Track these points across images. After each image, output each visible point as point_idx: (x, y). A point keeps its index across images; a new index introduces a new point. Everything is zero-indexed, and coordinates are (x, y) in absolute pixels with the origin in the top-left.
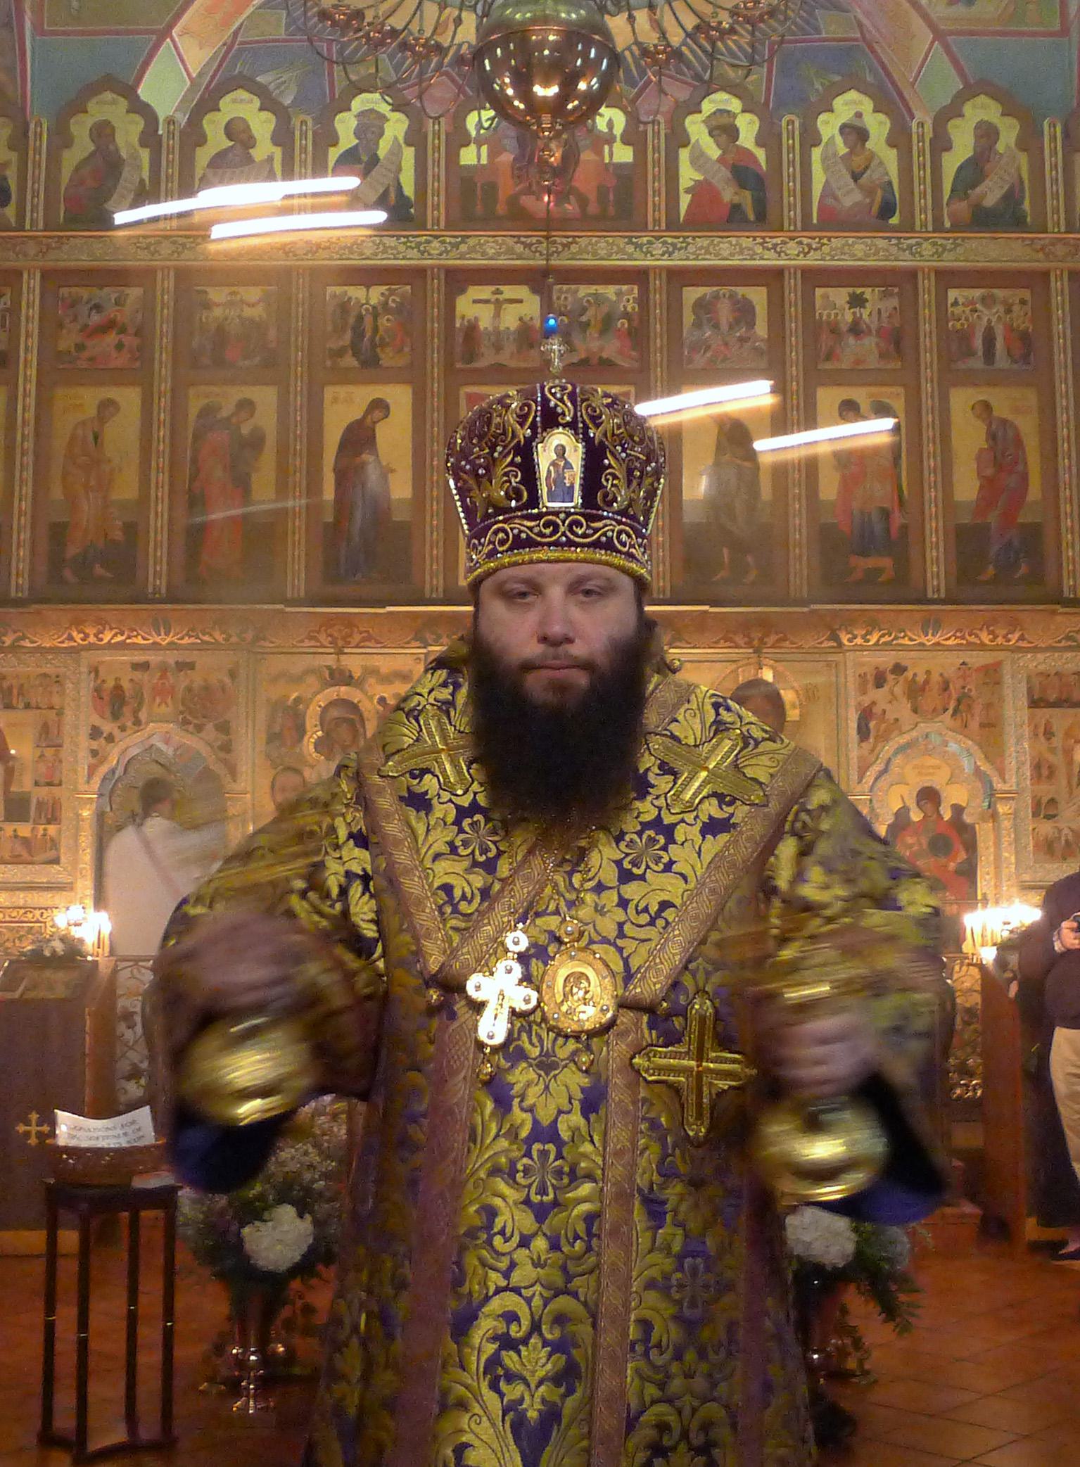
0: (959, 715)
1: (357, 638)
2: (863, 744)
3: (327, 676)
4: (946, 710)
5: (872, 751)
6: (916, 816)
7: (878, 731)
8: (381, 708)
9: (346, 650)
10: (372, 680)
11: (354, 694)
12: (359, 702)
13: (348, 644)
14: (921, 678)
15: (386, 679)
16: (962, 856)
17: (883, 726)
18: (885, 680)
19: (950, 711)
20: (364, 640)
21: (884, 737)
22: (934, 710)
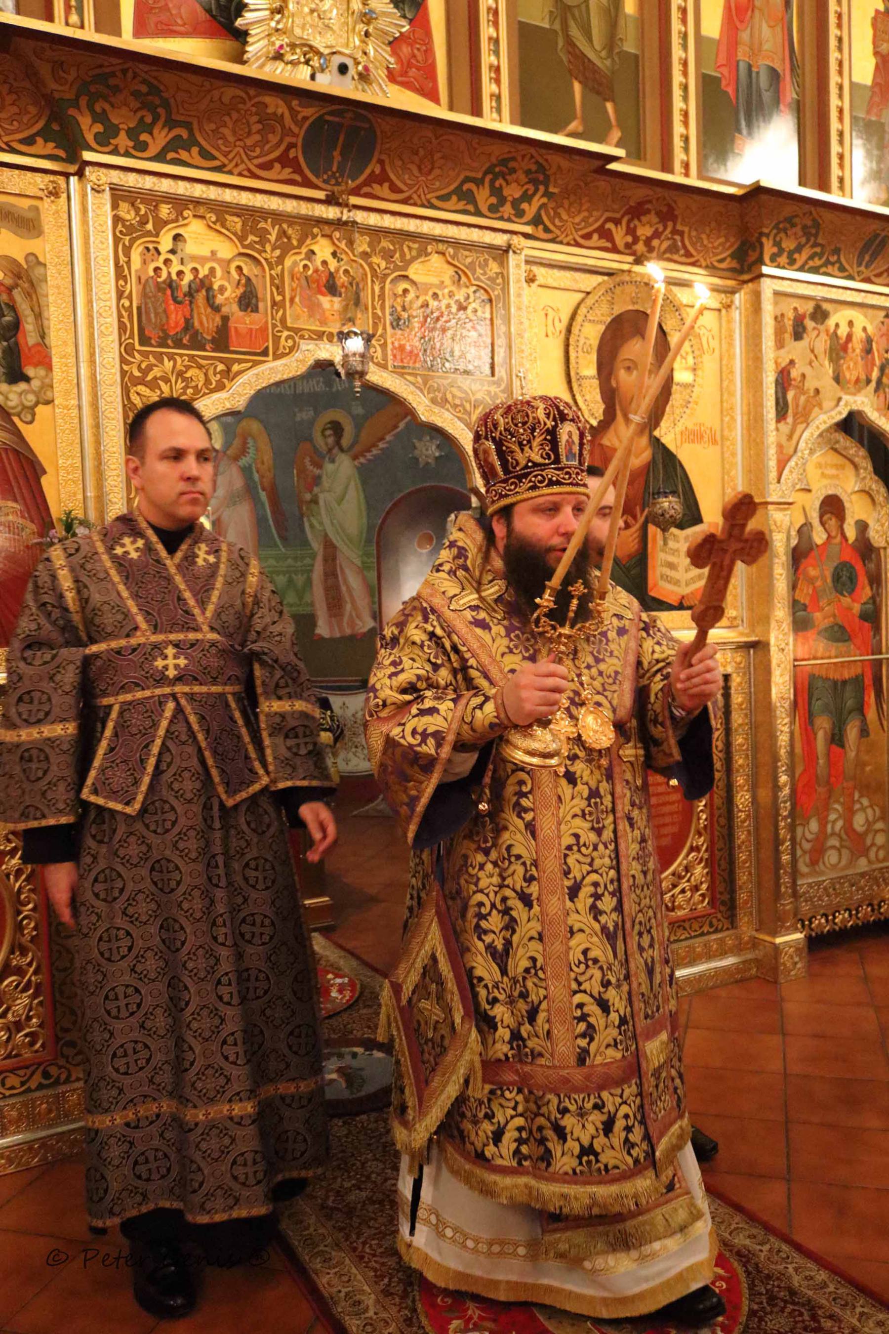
0: (881, 391)
2: (782, 425)
4: (868, 381)
5: (790, 437)
6: (819, 536)
7: (797, 406)
14: (843, 331)
16: (867, 592)
17: (803, 399)
18: (804, 329)
19: (873, 384)
21: (804, 417)
22: (857, 381)
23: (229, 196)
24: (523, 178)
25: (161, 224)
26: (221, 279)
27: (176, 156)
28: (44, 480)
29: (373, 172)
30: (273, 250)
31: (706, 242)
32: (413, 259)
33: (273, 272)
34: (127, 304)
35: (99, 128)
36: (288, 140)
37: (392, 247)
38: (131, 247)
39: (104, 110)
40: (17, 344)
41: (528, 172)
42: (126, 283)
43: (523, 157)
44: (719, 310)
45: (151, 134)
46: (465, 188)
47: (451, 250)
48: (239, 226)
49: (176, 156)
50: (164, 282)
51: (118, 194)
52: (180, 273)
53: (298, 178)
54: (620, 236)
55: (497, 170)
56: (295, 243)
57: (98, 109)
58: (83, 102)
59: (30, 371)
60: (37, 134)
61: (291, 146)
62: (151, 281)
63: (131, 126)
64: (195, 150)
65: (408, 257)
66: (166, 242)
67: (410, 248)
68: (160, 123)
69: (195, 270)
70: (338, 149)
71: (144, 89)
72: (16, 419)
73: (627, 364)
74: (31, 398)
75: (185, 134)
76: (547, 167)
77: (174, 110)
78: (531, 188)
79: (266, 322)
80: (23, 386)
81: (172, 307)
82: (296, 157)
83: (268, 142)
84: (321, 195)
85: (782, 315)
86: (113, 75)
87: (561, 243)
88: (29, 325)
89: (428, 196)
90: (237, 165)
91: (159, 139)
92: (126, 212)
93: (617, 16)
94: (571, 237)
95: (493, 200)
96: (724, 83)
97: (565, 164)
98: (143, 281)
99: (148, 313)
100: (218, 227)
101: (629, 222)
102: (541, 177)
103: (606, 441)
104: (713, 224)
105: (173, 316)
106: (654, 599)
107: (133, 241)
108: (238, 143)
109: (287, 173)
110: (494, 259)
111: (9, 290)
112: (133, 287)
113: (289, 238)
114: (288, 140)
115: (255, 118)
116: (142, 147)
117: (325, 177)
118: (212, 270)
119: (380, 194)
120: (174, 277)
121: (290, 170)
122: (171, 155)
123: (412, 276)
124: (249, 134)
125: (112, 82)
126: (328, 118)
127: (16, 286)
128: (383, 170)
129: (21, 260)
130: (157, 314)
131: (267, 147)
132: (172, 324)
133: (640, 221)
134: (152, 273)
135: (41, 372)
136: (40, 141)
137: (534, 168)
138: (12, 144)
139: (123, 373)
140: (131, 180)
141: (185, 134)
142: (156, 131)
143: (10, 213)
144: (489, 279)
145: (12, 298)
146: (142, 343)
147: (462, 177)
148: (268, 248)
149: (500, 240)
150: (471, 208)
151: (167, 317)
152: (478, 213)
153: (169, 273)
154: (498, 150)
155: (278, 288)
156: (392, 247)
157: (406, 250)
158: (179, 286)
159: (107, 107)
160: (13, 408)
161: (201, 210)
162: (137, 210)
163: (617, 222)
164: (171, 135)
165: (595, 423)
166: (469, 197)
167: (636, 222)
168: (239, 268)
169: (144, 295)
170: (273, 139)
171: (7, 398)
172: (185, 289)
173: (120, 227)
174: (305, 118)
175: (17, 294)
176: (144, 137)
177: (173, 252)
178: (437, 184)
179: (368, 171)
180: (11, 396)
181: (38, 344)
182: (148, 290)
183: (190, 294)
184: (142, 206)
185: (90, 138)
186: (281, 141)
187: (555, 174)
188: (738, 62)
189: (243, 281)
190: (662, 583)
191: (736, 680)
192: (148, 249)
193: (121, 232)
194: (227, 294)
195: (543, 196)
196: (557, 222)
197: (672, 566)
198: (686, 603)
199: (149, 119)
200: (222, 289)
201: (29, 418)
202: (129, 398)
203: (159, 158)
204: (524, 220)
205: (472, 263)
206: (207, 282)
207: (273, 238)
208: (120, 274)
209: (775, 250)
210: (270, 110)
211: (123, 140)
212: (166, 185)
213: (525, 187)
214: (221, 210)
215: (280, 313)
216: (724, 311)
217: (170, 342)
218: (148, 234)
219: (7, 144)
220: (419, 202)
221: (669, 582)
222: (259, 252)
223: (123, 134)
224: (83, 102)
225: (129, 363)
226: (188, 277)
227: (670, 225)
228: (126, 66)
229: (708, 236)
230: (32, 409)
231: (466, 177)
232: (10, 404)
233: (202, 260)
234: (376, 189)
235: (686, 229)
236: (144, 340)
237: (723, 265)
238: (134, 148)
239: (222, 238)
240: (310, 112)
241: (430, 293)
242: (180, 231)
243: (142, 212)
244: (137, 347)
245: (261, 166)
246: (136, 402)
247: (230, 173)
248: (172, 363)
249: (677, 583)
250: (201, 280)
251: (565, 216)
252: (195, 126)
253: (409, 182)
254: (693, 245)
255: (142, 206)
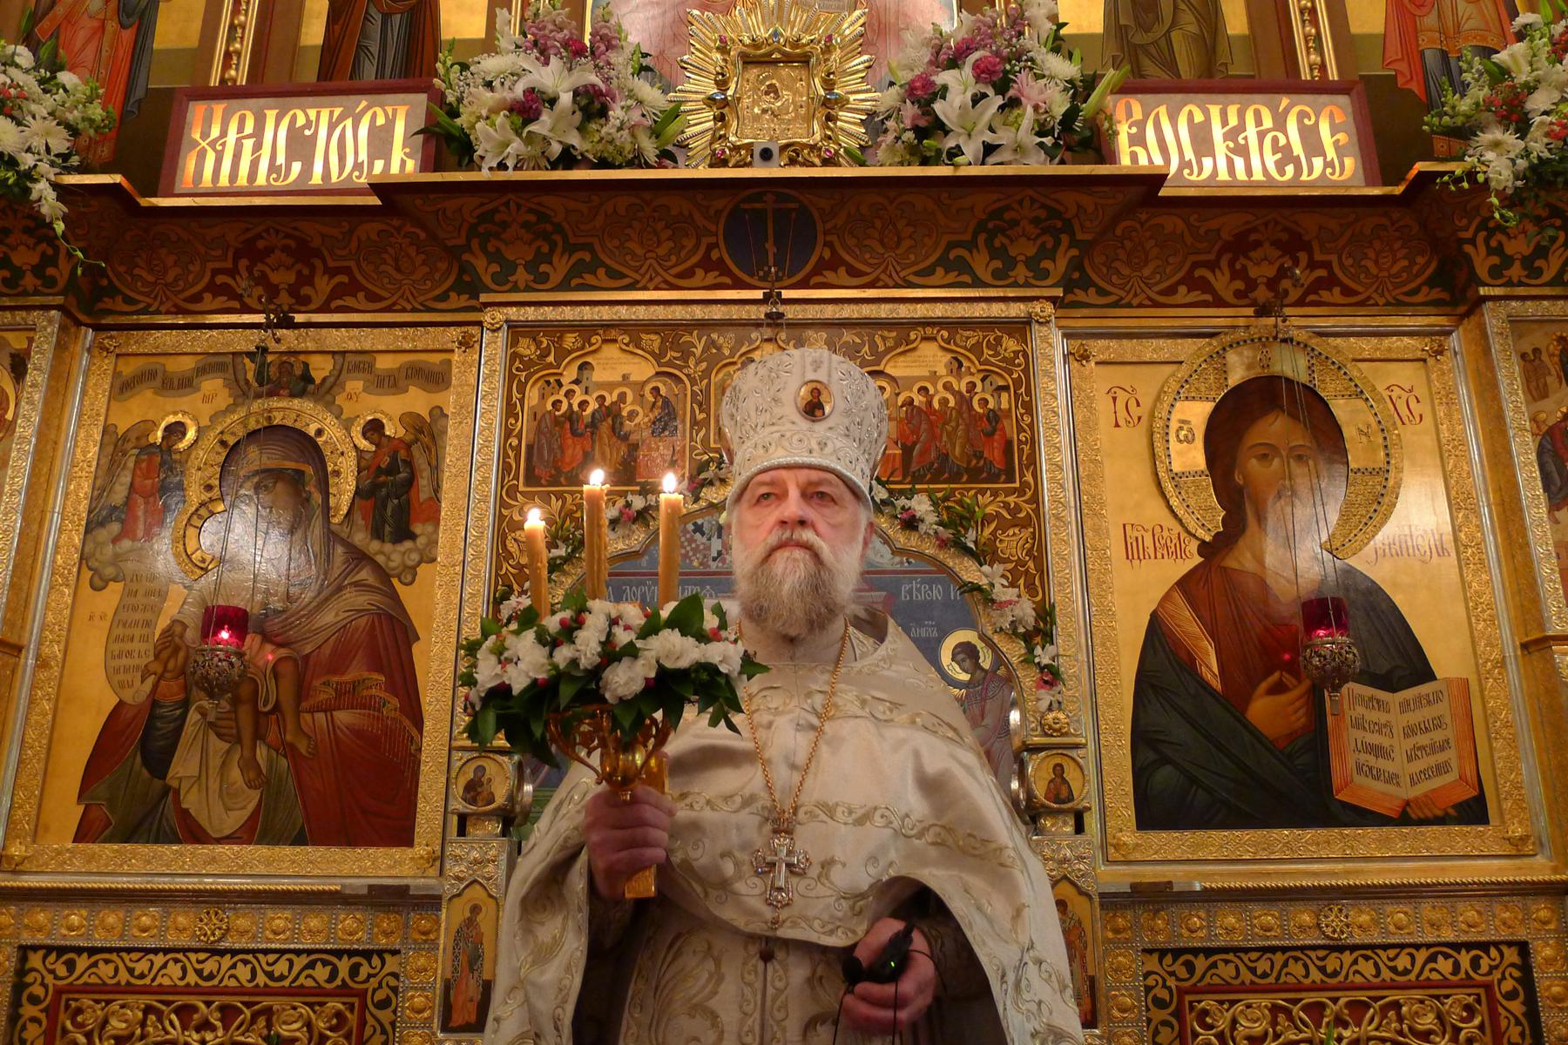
1: (323, 285)
3: (250, 376)
8: (364, 444)
9: (299, 318)
10: (355, 385)
11: (309, 416)
12: (320, 432)
13: (303, 303)
15: (390, 383)
20: (337, 292)
23: (641, 313)
24: (1032, 230)
25: (562, 354)
26: (632, 404)
27: (581, 281)
28: (416, 649)
29: (821, 258)
30: (697, 364)
31: (1374, 271)
32: (888, 350)
33: (695, 388)
34: (515, 442)
35: (495, 268)
36: (705, 241)
37: (858, 340)
38: (526, 382)
39: (498, 250)
40: (408, 501)
41: (1035, 221)
42: (517, 421)
43: (1020, 203)
44: (1424, 360)
45: (551, 263)
46: (952, 256)
47: (945, 334)
48: (656, 345)
49: (581, 281)
50: (562, 415)
51: (516, 330)
52: (583, 404)
53: (728, 280)
54: (1221, 282)
55: (990, 225)
56: (727, 352)
57: (491, 249)
58: (475, 244)
59: (417, 528)
60: (450, 289)
61: (710, 248)
62: (547, 416)
63: (529, 258)
64: (601, 272)
65: (881, 348)
66: (570, 374)
67: (884, 339)
68: (559, 250)
69: (602, 398)
70: (771, 240)
71: (532, 218)
72: (395, 581)
73: (1263, 451)
74: (415, 557)
75: (587, 257)
76: (1062, 209)
77: (570, 234)
78: (1049, 241)
79: (684, 446)
80: (408, 544)
81: (570, 441)
82: (721, 260)
83: (683, 247)
84: (758, 294)
85: (1536, 351)
86: (495, 210)
87: (1129, 306)
88: (423, 482)
89: (902, 274)
90: (651, 279)
91: (561, 266)
92: (526, 348)
93: (1215, 39)
94: (1144, 296)
95: (997, 264)
96: (1401, 81)
97: (1086, 200)
98: (538, 417)
99: (540, 449)
100: (631, 348)
101: (1231, 264)
102: (1059, 224)
103: (1231, 563)
104: (1377, 244)
105: (569, 452)
106: (1344, 805)
107: (527, 379)
108: (648, 255)
109: (712, 277)
110: (1010, 336)
111: (409, 446)
112: (524, 424)
113: (719, 348)
114: (705, 241)
115: (660, 225)
116: (542, 279)
117: (761, 273)
118: (622, 397)
119: (836, 282)
120: (576, 408)
121: (717, 273)
122: (574, 282)
123: (888, 370)
124: (659, 244)
125: (497, 217)
126: (742, 206)
127: (417, 440)
128: (834, 252)
129: (425, 414)
130: (551, 450)
131: (683, 254)
132: (567, 460)
133: (1250, 259)
134: (549, 407)
135: (429, 528)
136: (453, 295)
137: (1042, 214)
138: (427, 303)
139: (501, 517)
140: (531, 314)
141: (587, 257)
142: (555, 260)
143: (421, 369)
144: (1004, 360)
145: (409, 453)
146: (528, 483)
147: (943, 244)
148: (692, 362)
149: (1016, 310)
150: (967, 279)
151: (563, 452)
152: (978, 283)
153: (570, 405)
154: (982, 202)
155: (700, 405)
156: (858, 340)
157: (878, 340)
158: (580, 417)
159: (503, 247)
160: (393, 569)
161: (613, 334)
162: (538, 344)
163: (1213, 266)
164: (573, 260)
165: (1208, 539)
166: (963, 267)
167: (1242, 260)
168: (656, 390)
169: (539, 431)
170: (689, 243)
171: (389, 559)
172: (588, 420)
173: (517, 364)
174: (718, 212)
175: (416, 450)
176: (543, 268)
177: (577, 382)
178: (912, 257)
179: (813, 260)
180: (395, 556)
181: (431, 499)
182: (543, 425)
183: (594, 424)
184: (544, 340)
185: (487, 280)
186: (697, 246)
187: (1077, 216)
188: (1422, 54)
189: (660, 403)
190: (1360, 780)
191: (1543, 952)
192: (548, 383)
193: (518, 369)
194: (637, 420)
195: (1070, 247)
196: (1114, 279)
197: (1378, 751)
198: (1414, 813)
199: (545, 249)
200: (632, 415)
201: (409, 578)
202: (504, 546)
203: (564, 286)
204: (1049, 282)
205: (979, 344)
206: (615, 408)
207: (698, 351)
208: (510, 411)
209: (1495, 260)
210: (674, 212)
211: (521, 275)
212: (568, 313)
213: (1039, 242)
214: (633, 329)
215: (702, 434)
216: (1431, 361)
217: (562, 480)
218: (550, 366)
219: (421, 304)
220: (891, 283)
221: (1377, 778)
222: (680, 368)
223: (521, 270)
224: (475, 244)
225: (508, 506)
226: (593, 406)
227: (1303, 257)
228: (504, 199)
229: (1376, 262)
230: (413, 570)
231: (949, 243)
232: (392, 564)
233: (610, 386)
234: (830, 276)
235: (1334, 259)
236: (531, 479)
237: (1419, 298)
238: (534, 281)
239: (637, 360)
240: (721, 203)
241: (915, 389)
242: (589, 359)
243: (544, 345)
244: (521, 488)
245: (680, 276)
246: (512, 550)
247: (645, 288)
248: (560, 502)
249: (1392, 778)
250: (607, 408)
251: (1126, 271)
252: (598, 248)
253: (871, 261)
254: (1353, 277)
255: (544, 340)
